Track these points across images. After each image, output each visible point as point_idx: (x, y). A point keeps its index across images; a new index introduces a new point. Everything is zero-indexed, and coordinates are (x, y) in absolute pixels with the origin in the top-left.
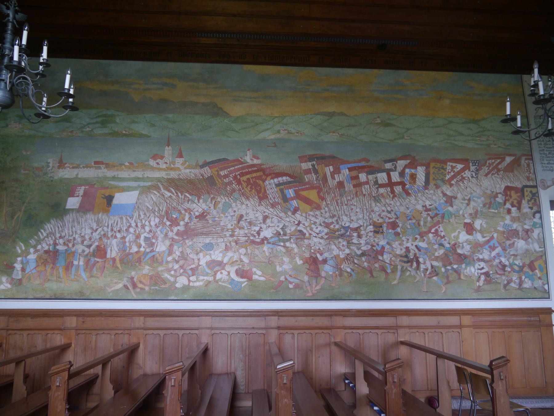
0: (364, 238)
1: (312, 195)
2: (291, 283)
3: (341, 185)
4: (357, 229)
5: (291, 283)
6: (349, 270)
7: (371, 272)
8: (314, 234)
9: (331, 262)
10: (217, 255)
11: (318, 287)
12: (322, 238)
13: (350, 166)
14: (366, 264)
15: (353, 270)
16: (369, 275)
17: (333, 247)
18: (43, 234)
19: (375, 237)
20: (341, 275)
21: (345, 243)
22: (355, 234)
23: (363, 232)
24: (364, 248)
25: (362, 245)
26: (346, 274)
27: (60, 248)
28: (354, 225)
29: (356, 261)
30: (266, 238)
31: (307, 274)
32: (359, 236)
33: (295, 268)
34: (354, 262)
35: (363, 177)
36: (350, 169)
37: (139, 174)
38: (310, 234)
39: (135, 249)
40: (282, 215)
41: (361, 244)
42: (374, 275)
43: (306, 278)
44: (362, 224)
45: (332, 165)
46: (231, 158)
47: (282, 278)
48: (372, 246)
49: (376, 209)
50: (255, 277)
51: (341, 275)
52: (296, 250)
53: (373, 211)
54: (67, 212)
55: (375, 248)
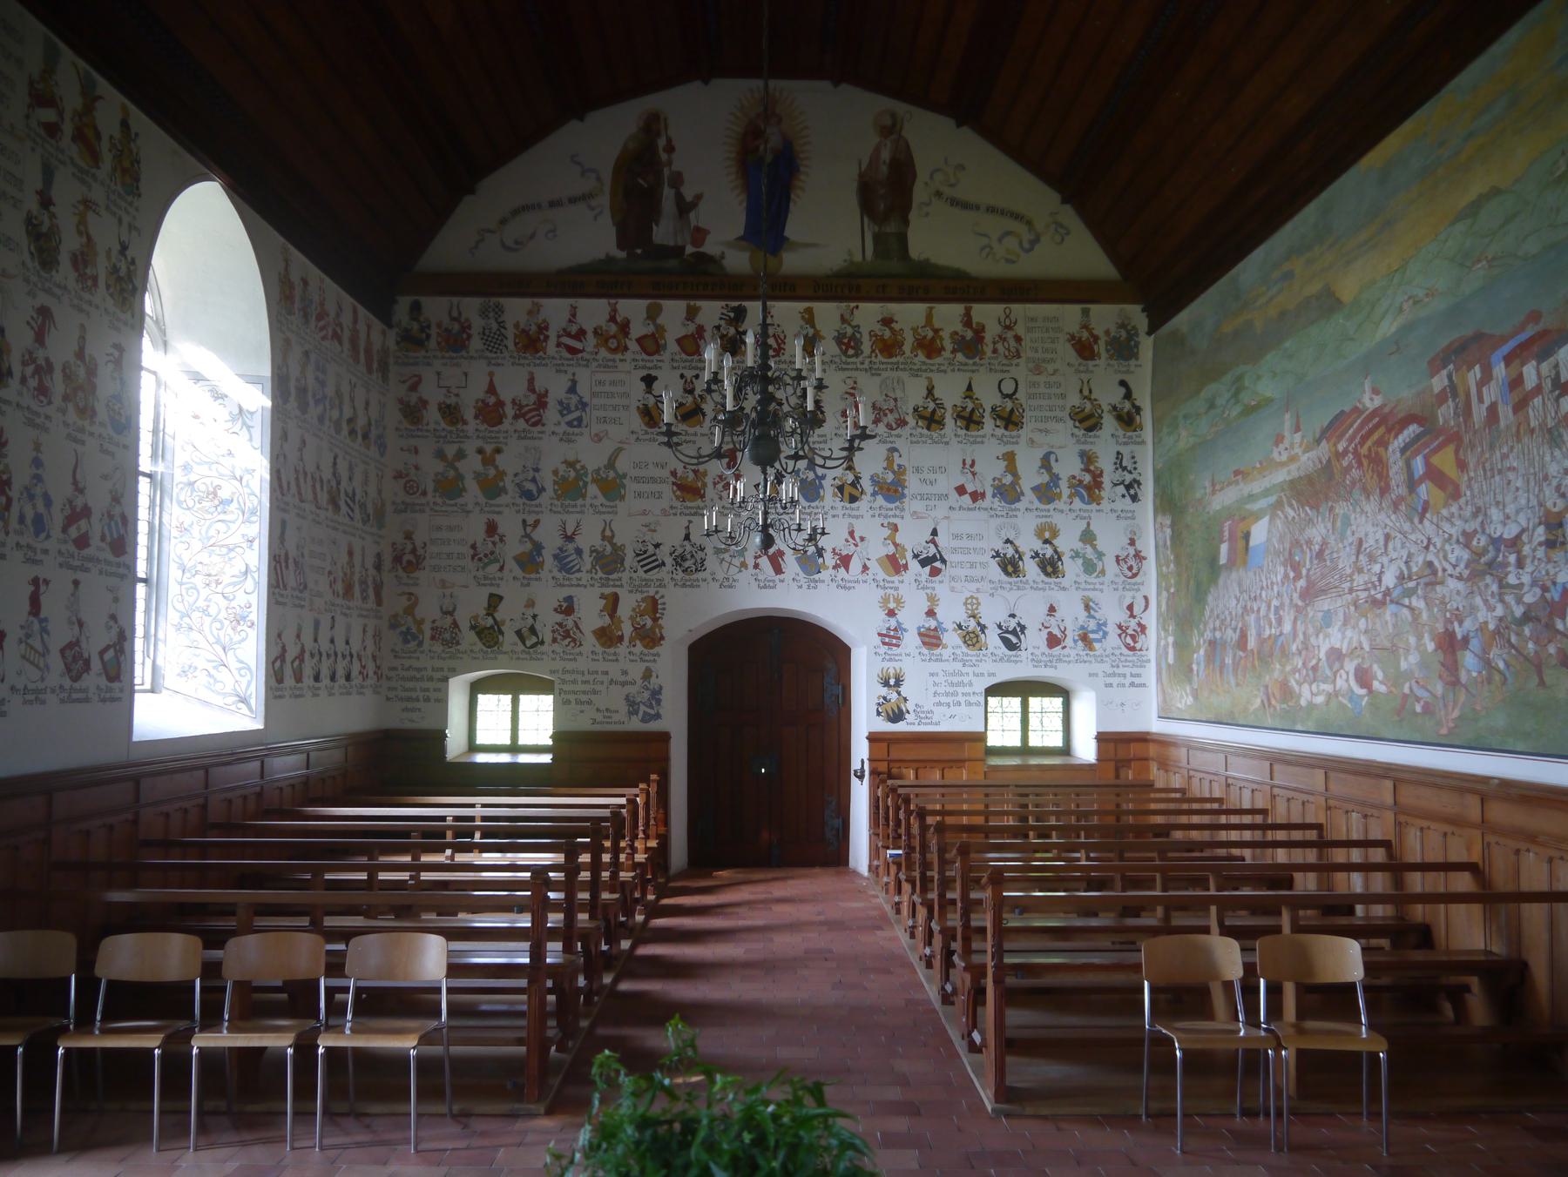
0: (1529, 568)
1: (1445, 460)
2: (1418, 699)
3: (1493, 410)
4: (1515, 543)
5: (1418, 699)
6: (1501, 665)
7: (1539, 670)
8: (1450, 570)
9: (1475, 644)
10: (1336, 638)
11: (1456, 714)
12: (1460, 578)
13: (1506, 349)
14: (1531, 645)
15: (1507, 665)
16: (1536, 680)
17: (1478, 601)
18: (1207, 613)
19: (1549, 560)
20: (1489, 680)
21: (1495, 588)
22: (1512, 558)
23: (1526, 550)
24: (1528, 599)
25: (1526, 589)
26: (1497, 677)
27: (1218, 635)
28: (1510, 532)
29: (1513, 639)
30: (1387, 592)
31: (1440, 677)
32: (1520, 564)
33: (1424, 664)
34: (1509, 641)
35: (1530, 372)
36: (1508, 360)
37: (1266, 483)
38: (1444, 570)
39: (1267, 633)
40: (1407, 527)
41: (1522, 584)
42: (1546, 679)
43: (1439, 688)
44: (1524, 524)
45: (1478, 361)
46: (1347, 409)
47: (1406, 690)
48: (1545, 589)
49: (1553, 469)
50: (1376, 685)
51: (1489, 680)
52: (1425, 616)
53: (1546, 478)
54: (1220, 567)
55: (1548, 595)
